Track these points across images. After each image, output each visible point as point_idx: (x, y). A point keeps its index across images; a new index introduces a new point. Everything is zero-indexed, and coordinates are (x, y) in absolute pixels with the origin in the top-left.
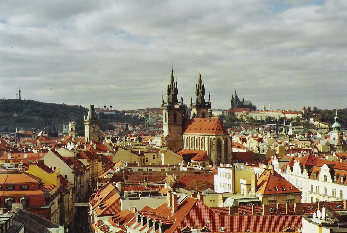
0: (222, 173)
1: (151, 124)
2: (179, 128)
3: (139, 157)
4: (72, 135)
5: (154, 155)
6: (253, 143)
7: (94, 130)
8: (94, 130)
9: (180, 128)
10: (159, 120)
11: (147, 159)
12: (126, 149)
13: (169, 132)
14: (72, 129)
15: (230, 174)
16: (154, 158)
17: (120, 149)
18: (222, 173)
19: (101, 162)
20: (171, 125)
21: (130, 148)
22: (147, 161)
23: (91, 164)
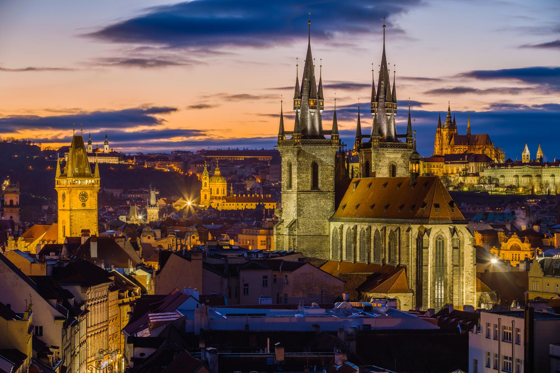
0: (492, 328)
1: (218, 193)
2: (325, 202)
3: (226, 281)
4: (11, 217)
5: (265, 277)
6: (519, 249)
7: (84, 205)
8: (84, 205)
9: (329, 204)
10: (238, 183)
11: (246, 285)
12: (189, 259)
13: (299, 215)
14: (11, 201)
15: (518, 330)
16: (265, 284)
17: (173, 256)
18: (492, 328)
19: (116, 292)
20: (303, 196)
21: (200, 257)
22: (246, 291)
23: (91, 296)
